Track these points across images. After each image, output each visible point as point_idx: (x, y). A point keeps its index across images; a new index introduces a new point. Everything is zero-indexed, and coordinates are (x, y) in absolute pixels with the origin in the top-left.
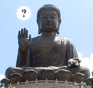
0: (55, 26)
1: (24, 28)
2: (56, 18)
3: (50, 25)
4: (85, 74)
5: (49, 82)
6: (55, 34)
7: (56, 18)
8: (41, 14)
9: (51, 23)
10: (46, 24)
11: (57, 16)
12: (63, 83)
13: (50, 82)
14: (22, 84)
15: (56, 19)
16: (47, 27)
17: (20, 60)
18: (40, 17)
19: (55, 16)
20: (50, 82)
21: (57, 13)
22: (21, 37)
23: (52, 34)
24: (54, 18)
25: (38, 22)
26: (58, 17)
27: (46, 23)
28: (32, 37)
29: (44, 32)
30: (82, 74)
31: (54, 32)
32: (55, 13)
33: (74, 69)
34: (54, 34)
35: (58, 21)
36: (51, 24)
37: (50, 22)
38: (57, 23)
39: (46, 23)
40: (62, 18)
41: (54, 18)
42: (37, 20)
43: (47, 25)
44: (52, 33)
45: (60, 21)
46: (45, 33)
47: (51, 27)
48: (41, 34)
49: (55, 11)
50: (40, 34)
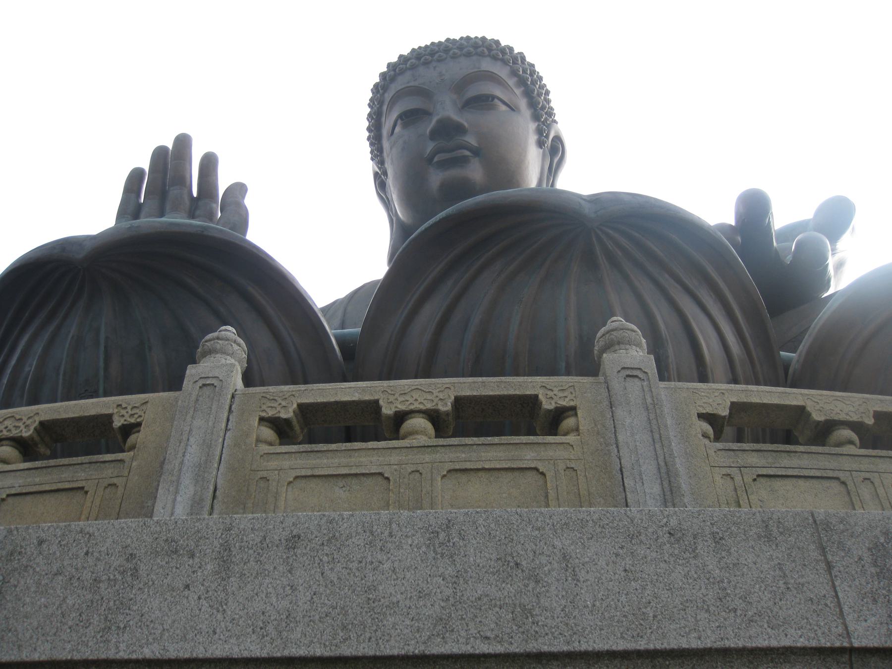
2: (513, 108)
3: (462, 161)
10: (430, 160)
12: (468, 420)
18: (385, 131)
19: (498, 92)
21: (514, 73)
24: (484, 102)
25: (381, 184)
32: (503, 72)
35: (540, 144)
36: (476, 152)
37: (460, 129)
39: (430, 146)
41: (484, 102)
42: (376, 175)
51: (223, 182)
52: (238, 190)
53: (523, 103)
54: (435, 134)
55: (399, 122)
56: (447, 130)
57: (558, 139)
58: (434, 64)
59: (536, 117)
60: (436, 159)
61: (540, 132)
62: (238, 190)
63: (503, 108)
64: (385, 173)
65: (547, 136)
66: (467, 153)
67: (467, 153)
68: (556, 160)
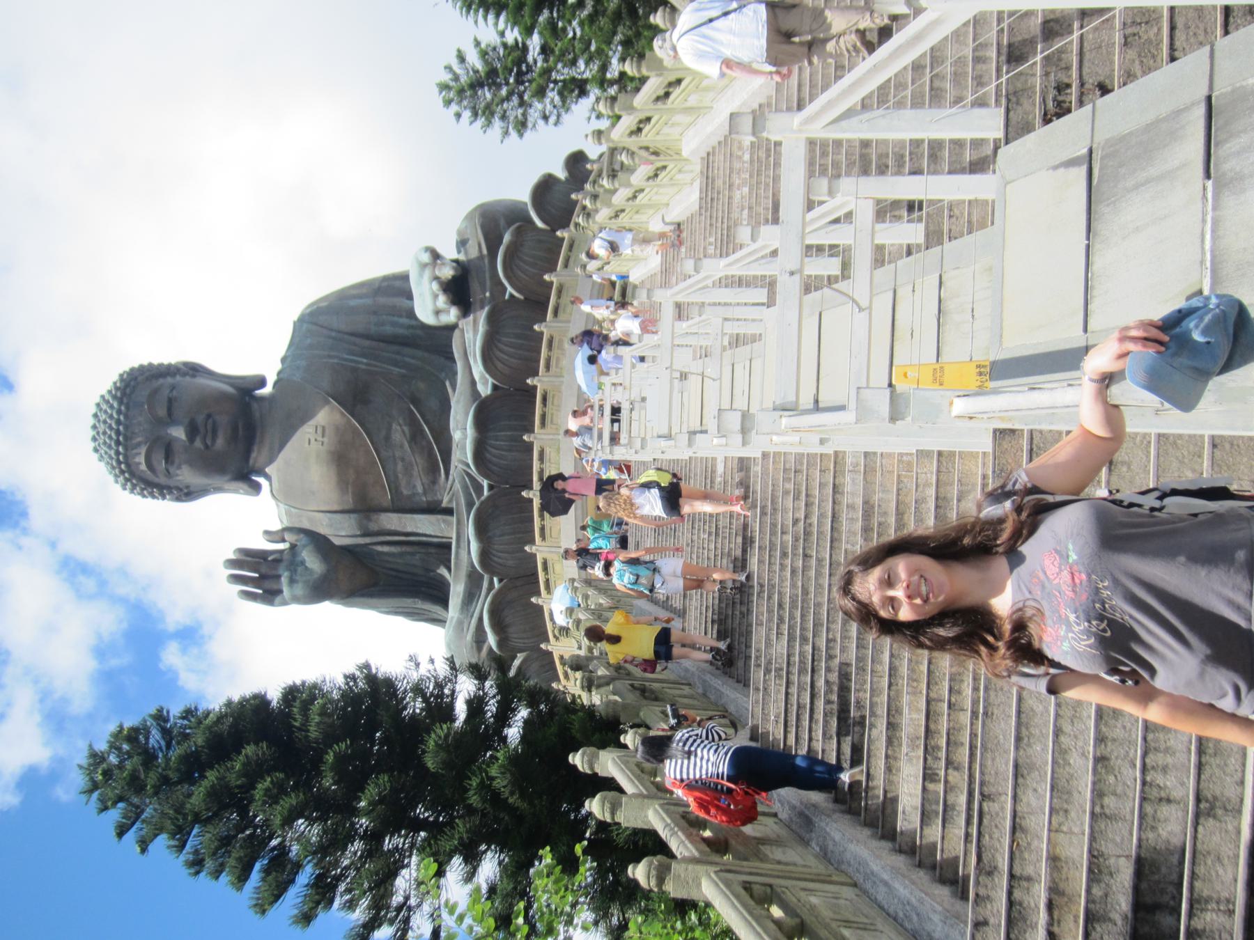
0: (223, 396)
2: (173, 388)
3: (214, 423)
4: (502, 223)
5: (543, 424)
6: (262, 399)
8: (149, 475)
9: (200, 419)
10: (207, 447)
11: (161, 381)
13: (543, 417)
14: (551, 577)
16: (220, 442)
17: (408, 602)
18: (162, 480)
19: (166, 392)
20: (543, 417)
22: (275, 587)
25: (186, 494)
26: (169, 380)
27: (198, 443)
28: (276, 526)
29: (251, 462)
30: (507, 238)
31: (255, 406)
33: (474, 286)
35: (194, 376)
36: (209, 416)
38: (201, 381)
42: (178, 499)
43: (213, 444)
44: (257, 415)
45: (194, 370)
46: (254, 455)
47: (223, 420)
48: (261, 480)
49: (133, 392)
50: (257, 488)
56: (193, 431)
57: (186, 364)
58: (129, 434)
60: (209, 443)
61: (185, 375)
63: (175, 393)
64: (187, 487)
67: (210, 421)
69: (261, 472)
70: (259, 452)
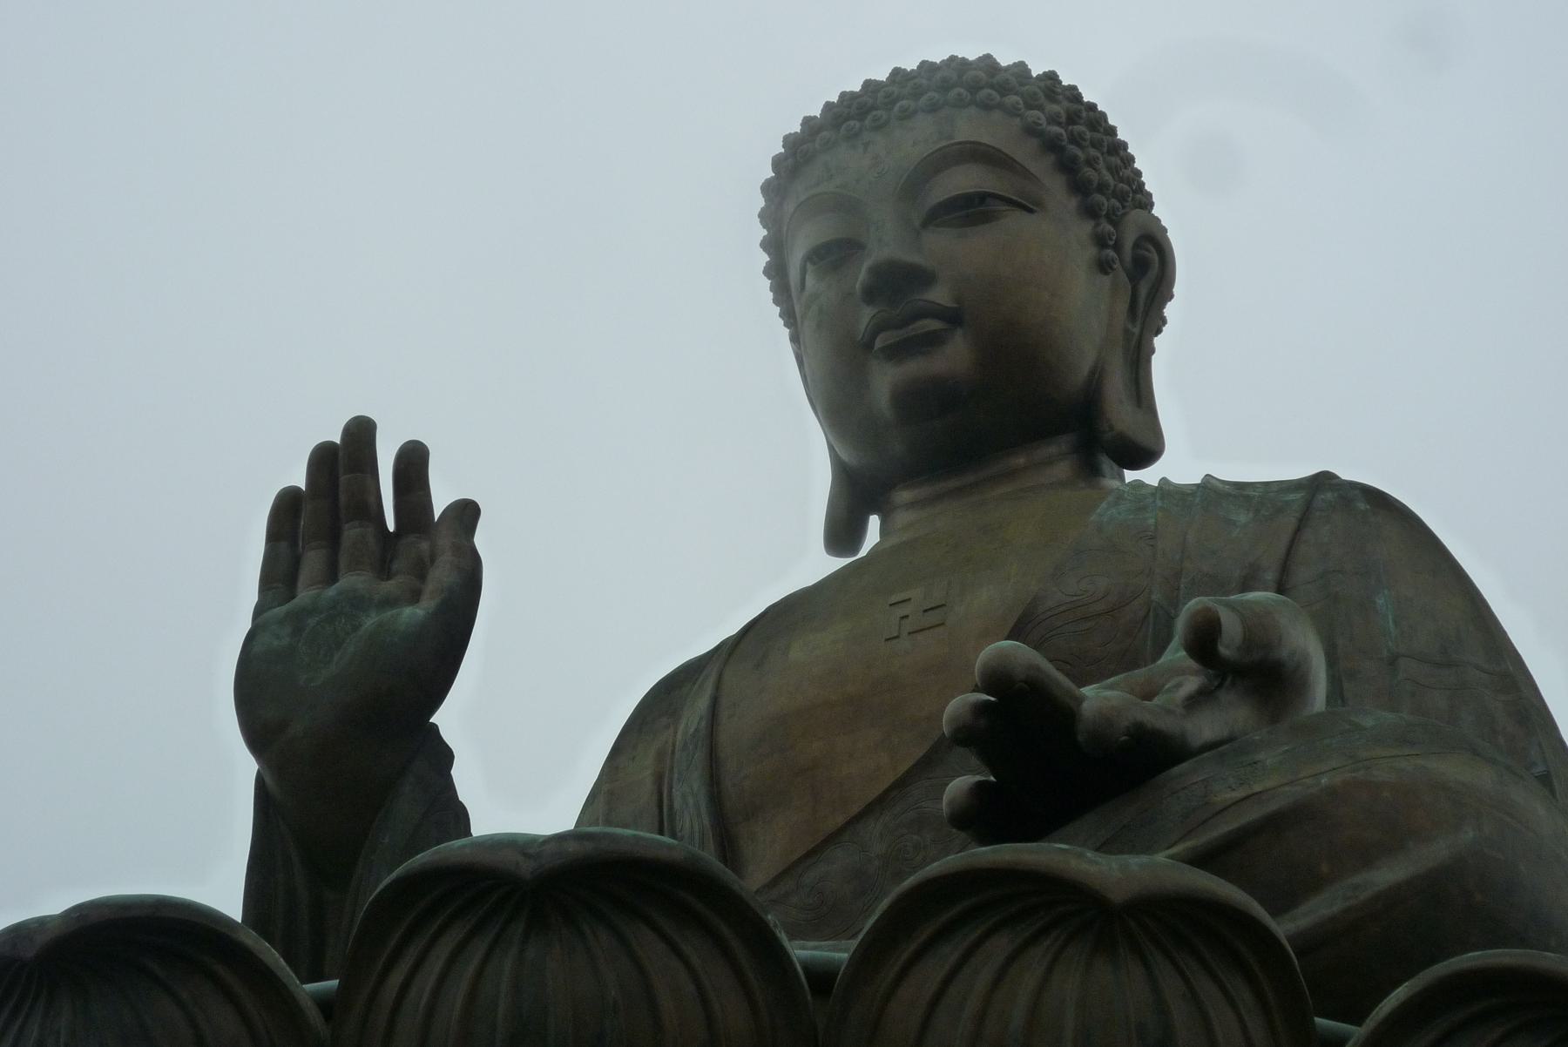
1: (361, 433)
3: (931, 342)
6: (1090, 471)
7: (1027, 206)
9: (939, 295)
10: (868, 346)
15: (1015, 221)
16: (884, 380)
23: (1011, 474)
29: (903, 496)
31: (1059, 446)
34: (1063, 470)
35: (1103, 267)
36: (954, 318)
37: (918, 277)
39: (866, 316)
40: (1173, 207)
44: (1021, 461)
49: (987, 107)
51: (440, 501)
52: (466, 513)
53: (1054, 187)
54: (870, 295)
55: (810, 267)
56: (895, 284)
59: (1090, 212)
60: (878, 344)
61: (1101, 241)
62: (466, 513)
65: (1117, 247)
66: (933, 325)
67: (933, 325)
68: (1143, 291)
69: (884, 531)
70: (912, 505)
